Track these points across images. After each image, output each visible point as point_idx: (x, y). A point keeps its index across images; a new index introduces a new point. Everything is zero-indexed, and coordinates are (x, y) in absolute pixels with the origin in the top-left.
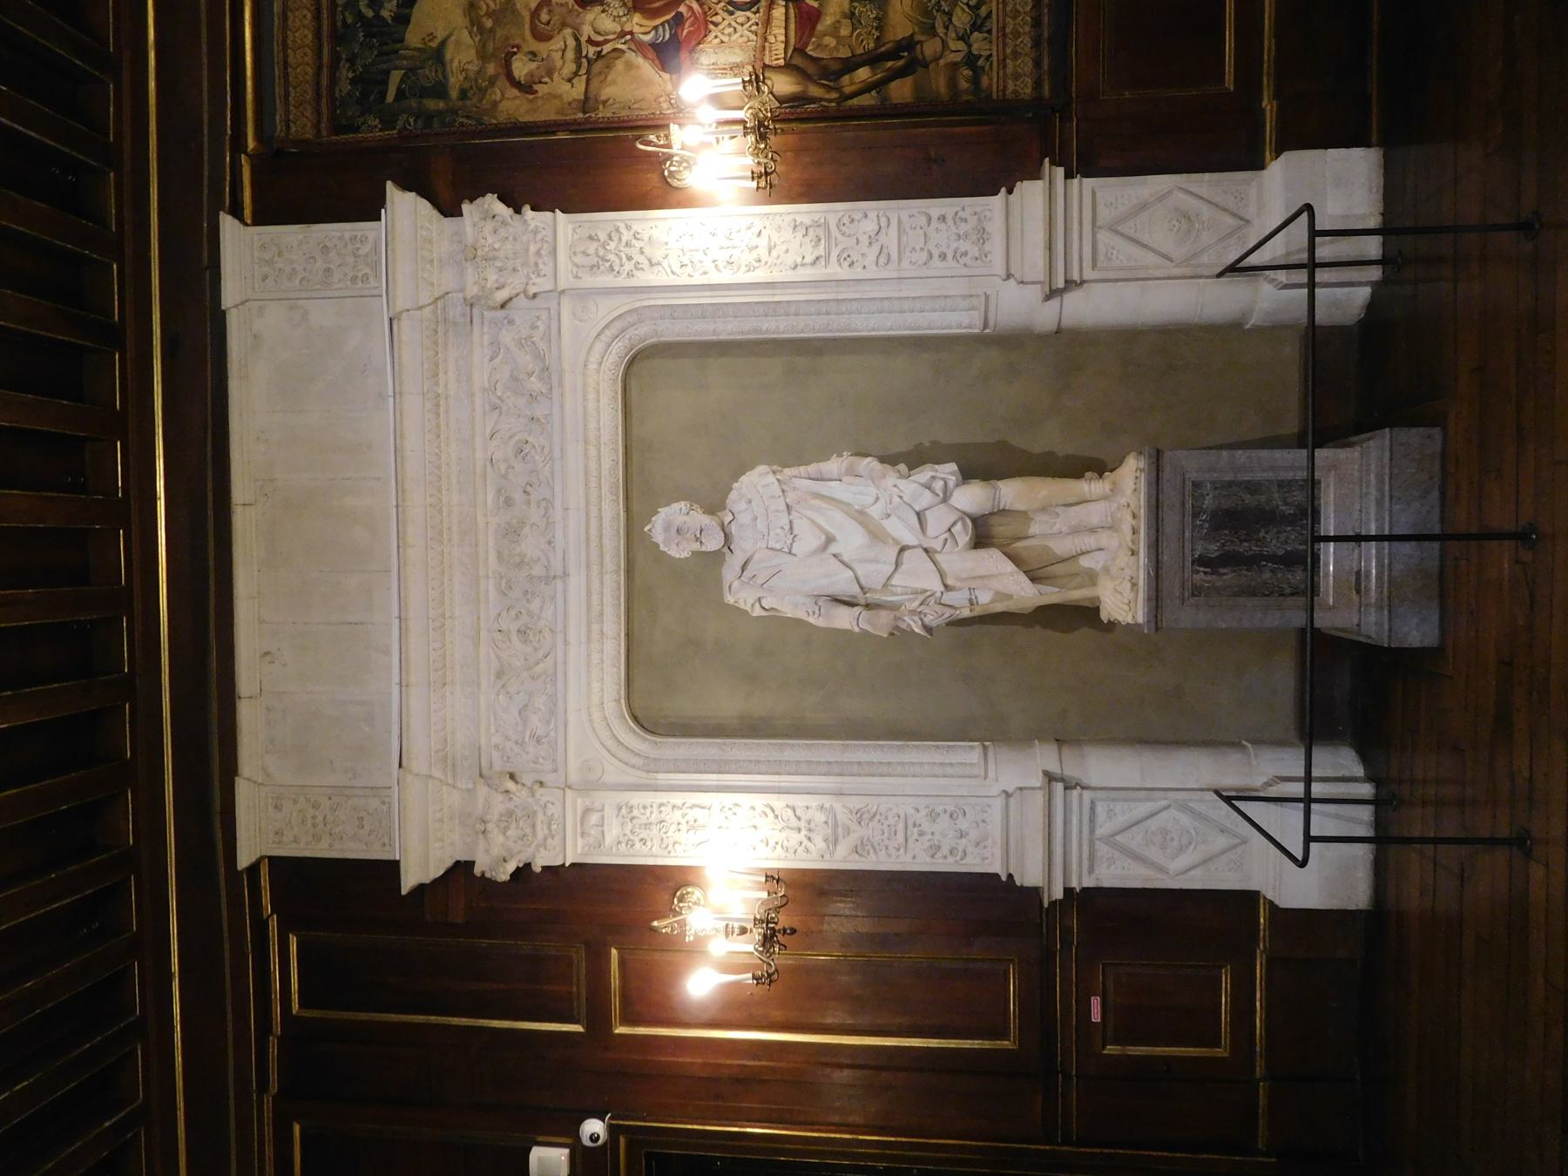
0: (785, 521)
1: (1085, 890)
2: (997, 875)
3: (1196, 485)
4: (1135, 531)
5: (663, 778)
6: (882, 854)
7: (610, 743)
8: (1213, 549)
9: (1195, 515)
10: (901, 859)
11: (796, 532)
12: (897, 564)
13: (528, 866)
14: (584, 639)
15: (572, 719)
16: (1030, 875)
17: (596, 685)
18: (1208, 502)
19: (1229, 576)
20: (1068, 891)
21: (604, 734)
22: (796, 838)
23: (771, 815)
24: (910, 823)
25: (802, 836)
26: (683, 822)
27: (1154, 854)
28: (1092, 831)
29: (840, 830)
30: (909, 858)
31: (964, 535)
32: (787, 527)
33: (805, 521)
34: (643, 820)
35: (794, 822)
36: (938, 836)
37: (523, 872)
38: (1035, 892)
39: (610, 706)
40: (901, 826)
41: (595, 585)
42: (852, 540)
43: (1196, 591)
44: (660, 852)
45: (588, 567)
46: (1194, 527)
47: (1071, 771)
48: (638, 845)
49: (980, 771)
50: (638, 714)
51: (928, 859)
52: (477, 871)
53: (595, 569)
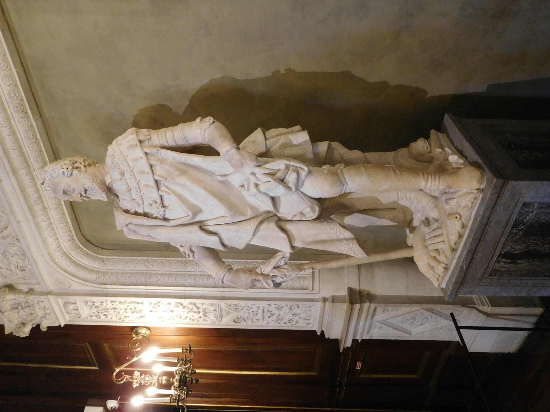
0: (155, 195)
1: (363, 340)
2: (315, 332)
3: (525, 205)
4: (460, 236)
5: (110, 288)
6: (249, 322)
7: (72, 268)
8: (519, 248)
9: (515, 226)
10: (258, 324)
11: (166, 204)
12: (254, 234)
13: (38, 326)
14: (30, 218)
15: (39, 260)
16: (334, 332)
17: (50, 240)
18: (530, 217)
19: (523, 264)
20: (355, 341)
21: (65, 264)
22: (196, 316)
23: (181, 307)
24: (266, 311)
25: (201, 314)
26: (128, 308)
27: (406, 326)
28: (372, 318)
29: (224, 313)
30: (265, 323)
31: (312, 213)
32: (159, 201)
33: (172, 196)
34: (103, 307)
35: (195, 309)
36: (282, 315)
37: (36, 329)
38: (336, 342)
39: (67, 246)
40: (260, 312)
41: (26, 181)
42: (213, 211)
43: (494, 273)
44: (117, 320)
45: (14, 171)
46: (510, 233)
47: (366, 287)
48: (103, 317)
49: (308, 283)
50: (89, 238)
51: (276, 324)
52: (7, 332)
53: (22, 173)
